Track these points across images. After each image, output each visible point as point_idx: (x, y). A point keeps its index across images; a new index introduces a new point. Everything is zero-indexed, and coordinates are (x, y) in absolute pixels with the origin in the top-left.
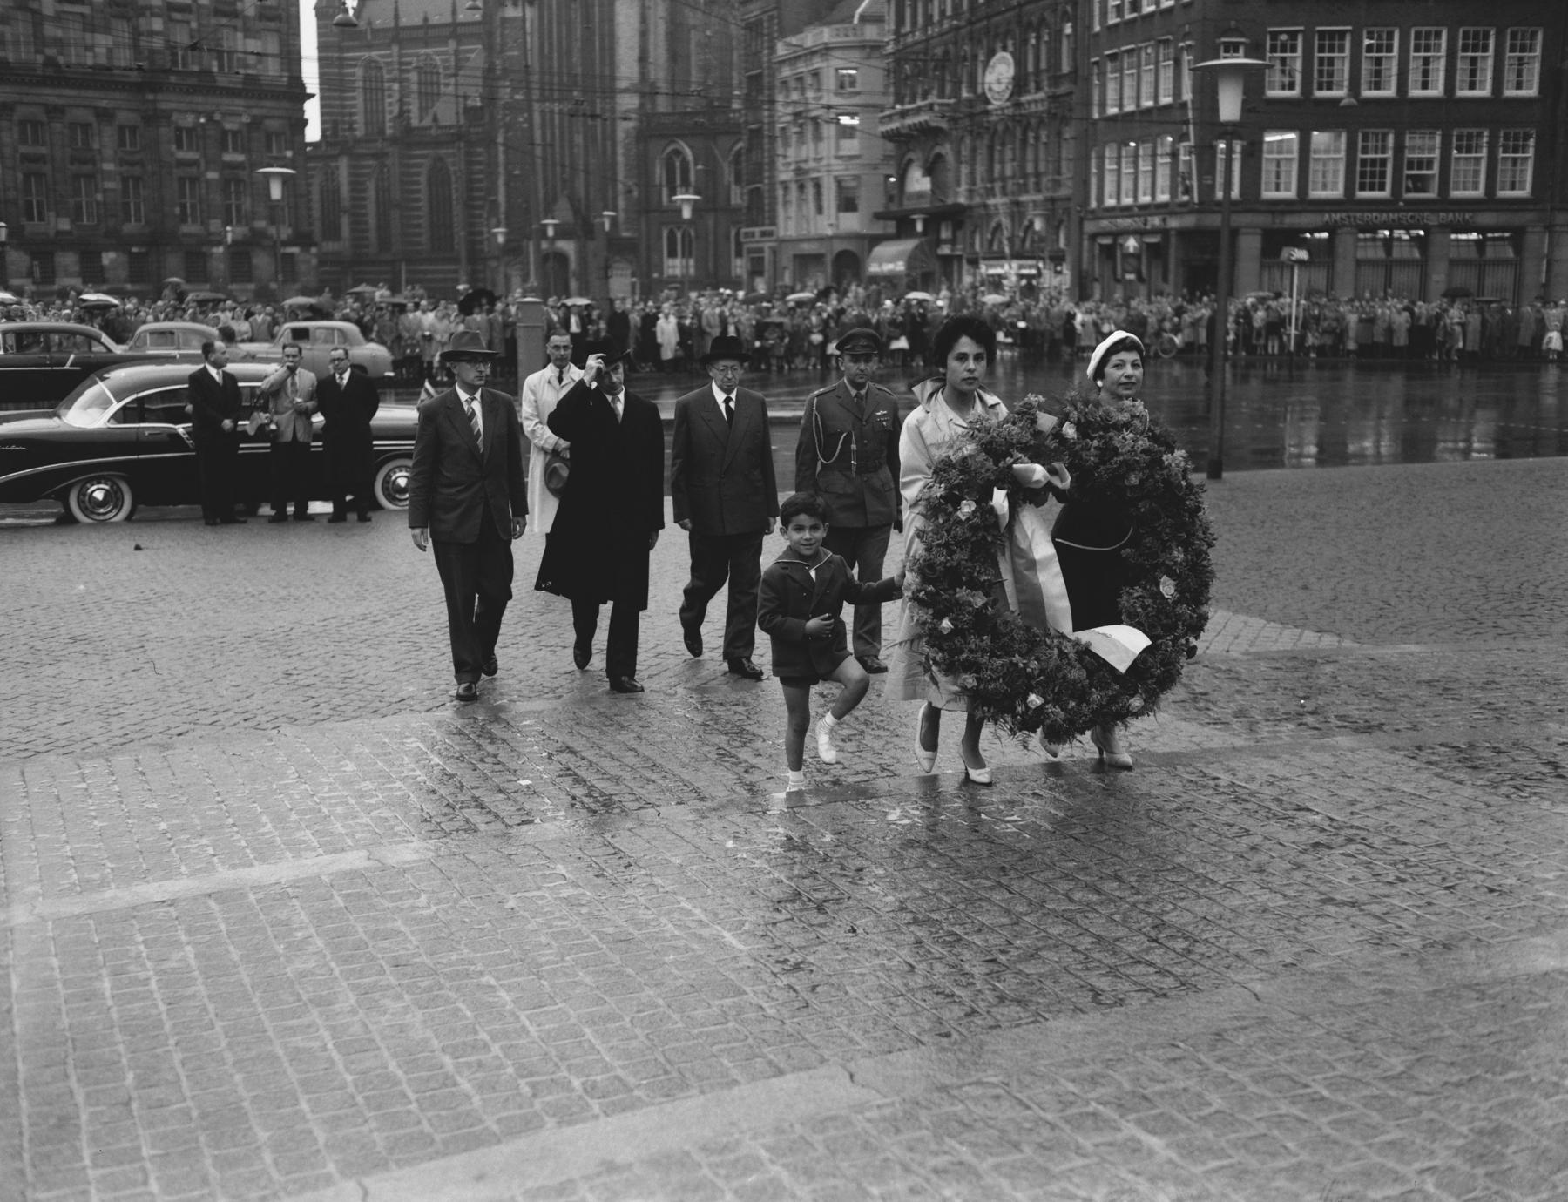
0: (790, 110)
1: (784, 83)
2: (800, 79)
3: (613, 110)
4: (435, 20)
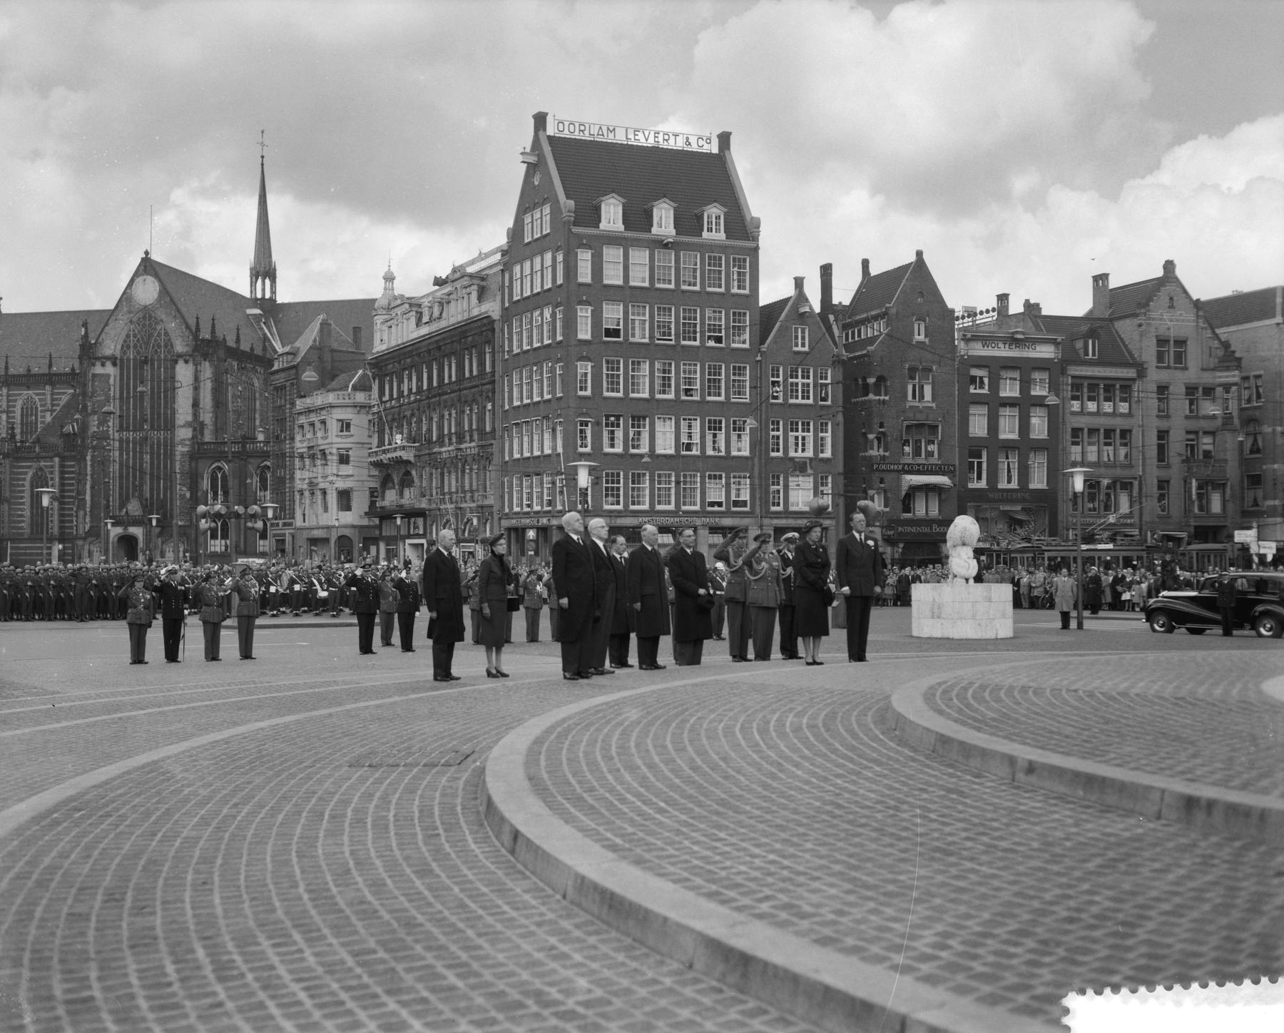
0: (305, 444)
1: (302, 427)
2: (312, 425)
3: (172, 438)
4: (35, 370)
